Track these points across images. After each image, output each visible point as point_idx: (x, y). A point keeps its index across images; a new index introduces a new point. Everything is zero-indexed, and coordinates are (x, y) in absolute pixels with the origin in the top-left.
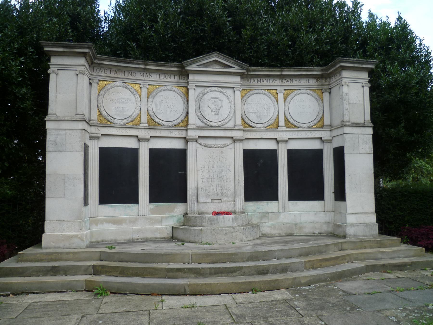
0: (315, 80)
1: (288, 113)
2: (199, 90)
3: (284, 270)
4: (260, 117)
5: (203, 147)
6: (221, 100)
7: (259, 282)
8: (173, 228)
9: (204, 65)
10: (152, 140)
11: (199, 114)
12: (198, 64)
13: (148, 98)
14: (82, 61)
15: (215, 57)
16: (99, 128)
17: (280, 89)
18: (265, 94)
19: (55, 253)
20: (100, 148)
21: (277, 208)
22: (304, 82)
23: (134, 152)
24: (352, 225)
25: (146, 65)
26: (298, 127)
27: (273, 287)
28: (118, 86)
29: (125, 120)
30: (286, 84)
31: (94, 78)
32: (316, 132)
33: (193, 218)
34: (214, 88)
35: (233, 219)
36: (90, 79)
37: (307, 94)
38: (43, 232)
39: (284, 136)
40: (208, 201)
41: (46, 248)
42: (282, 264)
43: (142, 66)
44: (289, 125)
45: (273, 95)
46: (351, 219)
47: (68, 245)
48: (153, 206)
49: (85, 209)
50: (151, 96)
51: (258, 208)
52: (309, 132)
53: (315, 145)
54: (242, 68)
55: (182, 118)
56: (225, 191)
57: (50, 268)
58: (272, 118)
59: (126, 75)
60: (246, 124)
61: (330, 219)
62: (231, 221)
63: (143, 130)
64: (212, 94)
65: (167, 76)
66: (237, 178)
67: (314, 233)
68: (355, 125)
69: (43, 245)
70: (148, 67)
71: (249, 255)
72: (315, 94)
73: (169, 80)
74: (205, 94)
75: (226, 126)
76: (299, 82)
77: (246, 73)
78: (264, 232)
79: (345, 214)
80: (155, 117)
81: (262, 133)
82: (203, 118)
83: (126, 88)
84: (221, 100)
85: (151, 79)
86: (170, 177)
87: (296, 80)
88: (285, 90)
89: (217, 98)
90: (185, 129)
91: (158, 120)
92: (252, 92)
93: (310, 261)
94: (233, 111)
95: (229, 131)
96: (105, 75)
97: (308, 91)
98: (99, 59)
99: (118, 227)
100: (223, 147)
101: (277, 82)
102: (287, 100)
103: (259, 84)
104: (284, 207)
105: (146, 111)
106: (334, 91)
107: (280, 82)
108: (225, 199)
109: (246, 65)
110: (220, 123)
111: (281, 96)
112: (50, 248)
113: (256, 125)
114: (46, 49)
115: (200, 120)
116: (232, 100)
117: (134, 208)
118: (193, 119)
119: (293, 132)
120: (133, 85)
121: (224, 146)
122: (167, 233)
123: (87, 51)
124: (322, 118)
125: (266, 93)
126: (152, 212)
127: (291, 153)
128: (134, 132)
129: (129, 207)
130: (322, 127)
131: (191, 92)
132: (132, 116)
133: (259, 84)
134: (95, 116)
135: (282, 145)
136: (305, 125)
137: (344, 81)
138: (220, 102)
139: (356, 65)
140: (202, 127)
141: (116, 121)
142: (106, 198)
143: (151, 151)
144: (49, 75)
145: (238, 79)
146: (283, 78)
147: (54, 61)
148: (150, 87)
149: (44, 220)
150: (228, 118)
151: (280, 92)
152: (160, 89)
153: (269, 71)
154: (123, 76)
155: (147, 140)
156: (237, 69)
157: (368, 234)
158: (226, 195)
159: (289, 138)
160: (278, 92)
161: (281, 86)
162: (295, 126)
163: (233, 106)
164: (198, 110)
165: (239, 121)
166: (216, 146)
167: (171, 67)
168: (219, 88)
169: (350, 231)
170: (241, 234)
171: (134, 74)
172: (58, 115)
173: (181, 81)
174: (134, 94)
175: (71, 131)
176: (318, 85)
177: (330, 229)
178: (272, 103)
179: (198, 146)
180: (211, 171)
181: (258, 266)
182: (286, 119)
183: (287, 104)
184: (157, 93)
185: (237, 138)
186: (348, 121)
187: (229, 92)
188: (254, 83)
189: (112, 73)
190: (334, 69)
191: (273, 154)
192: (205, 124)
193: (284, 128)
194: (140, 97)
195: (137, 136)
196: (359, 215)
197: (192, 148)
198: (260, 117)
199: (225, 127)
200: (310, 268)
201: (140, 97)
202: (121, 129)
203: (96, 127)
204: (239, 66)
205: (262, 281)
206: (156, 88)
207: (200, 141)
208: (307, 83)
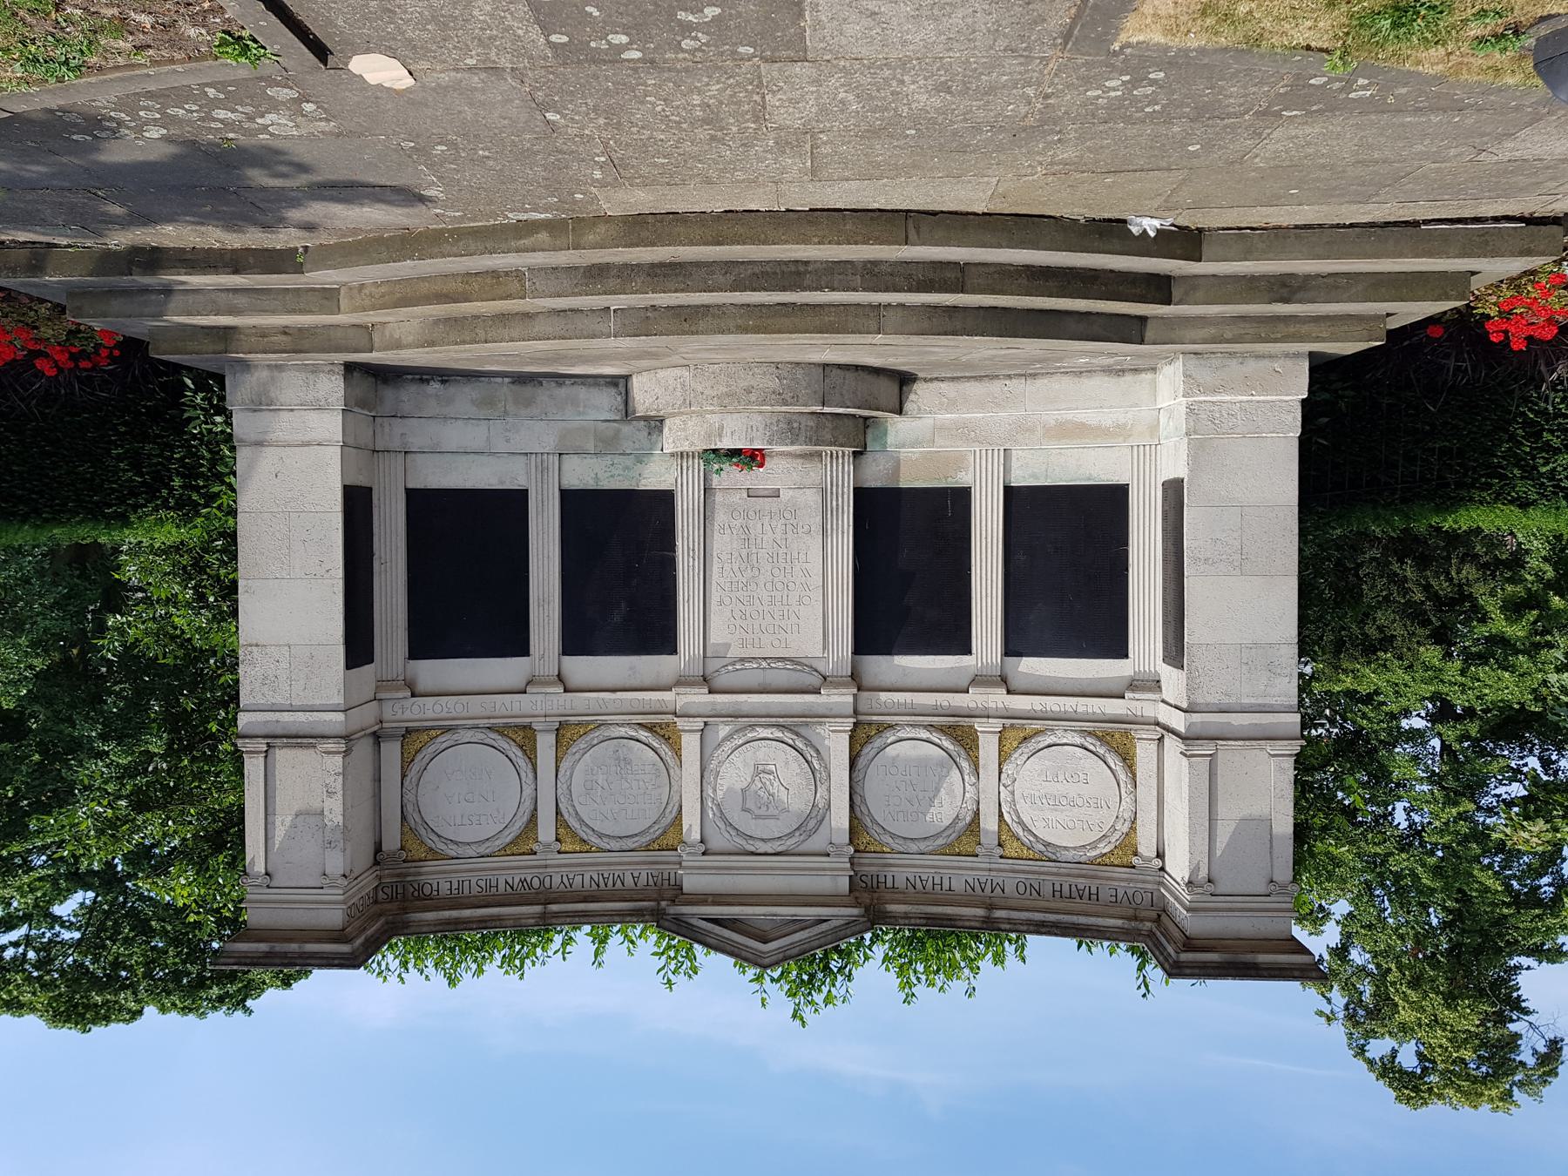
1: (523, 775)
2: (817, 842)
3: (596, 276)
4: (618, 759)
7: (691, 243)
8: (900, 411)
9: (799, 925)
12: (824, 927)
18: (600, 836)
19: (1276, 341)
20: (1127, 656)
21: (565, 467)
27: (639, 227)
29: (1049, 741)
32: (430, 714)
33: (841, 440)
34: (770, 851)
36: (1162, 869)
37: (456, 843)
41: (1297, 355)
42: (605, 293)
45: (574, 834)
46: (330, 425)
47: (1233, 363)
48: (962, 479)
49: (1181, 472)
50: (968, 819)
51: (627, 468)
52: (454, 714)
53: (432, 671)
55: (868, 751)
56: (737, 523)
57: (1298, 296)
61: (387, 430)
62: (727, 431)
64: (774, 828)
66: (698, 564)
67: (443, 382)
69: (1306, 365)
71: (702, 325)
73: (910, 873)
76: (482, 883)
77: (663, 904)
78: (613, 391)
79: (345, 445)
85: (970, 876)
86: (904, 567)
87: (494, 890)
89: (758, 817)
90: (861, 718)
91: (946, 743)
92: (644, 839)
93: (506, 298)
99: (1070, 417)
104: (544, 470)
105: (981, 771)
106: (366, 857)
111: (546, 832)
112: (1287, 355)
118: (837, 745)
122: (920, 395)
123: (1184, 957)
124: (406, 764)
127: (518, 645)
129: (1034, 476)
130: (408, 731)
136: (468, 735)
137: (336, 895)
139: (294, 947)
141: (1078, 740)
142: (1107, 504)
145: (691, 883)
149: (1304, 442)
152: (940, 841)
155: (979, 680)
160: (558, 846)
162: (501, 734)
165: (690, 743)
168: (752, 849)
170: (700, 389)
176: (420, 874)
177: (389, 393)
180: (780, 586)
181: (682, 291)
182: (530, 754)
183: (527, 806)
189: (1094, 890)
190: (369, 932)
191: (576, 641)
192: (797, 734)
194: (1001, 815)
195: (1009, 692)
196: (300, 437)
200: (507, 274)
205: (681, 244)
206: (951, 845)
207: (815, 680)
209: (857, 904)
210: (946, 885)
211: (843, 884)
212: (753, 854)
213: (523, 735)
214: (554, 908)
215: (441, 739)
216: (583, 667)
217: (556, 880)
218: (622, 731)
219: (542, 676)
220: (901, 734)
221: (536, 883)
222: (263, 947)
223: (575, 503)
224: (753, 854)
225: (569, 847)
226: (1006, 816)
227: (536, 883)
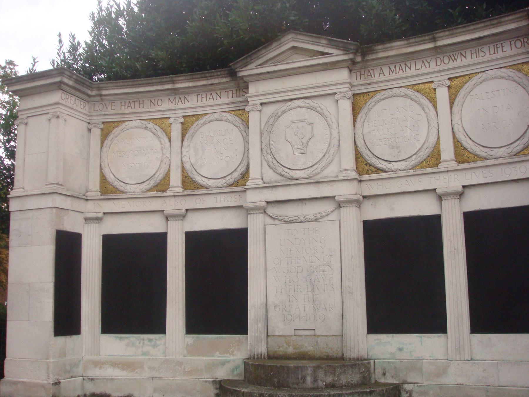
0: (519, 44)
1: (461, 130)
2: (269, 110)
4: (397, 147)
5: (277, 222)
6: (311, 124)
10: (190, 215)
11: (269, 157)
12: (259, 62)
13: (183, 140)
14: (56, 97)
15: (290, 41)
16: (100, 202)
17: (439, 79)
18: (406, 96)
22: (492, 52)
23: (159, 241)
25: (173, 82)
28: (132, 128)
30: (452, 64)
31: (95, 119)
34: (295, 101)
37: (502, 78)
44: (462, 155)
45: (425, 94)
48: (192, 338)
50: (187, 136)
54: (346, 50)
58: (425, 147)
60: (370, 165)
63: (173, 199)
64: (292, 116)
65: (214, 95)
72: (520, 75)
73: (219, 101)
74: (279, 117)
76: (482, 54)
80: (195, 172)
81: (404, 180)
82: (277, 164)
83: (146, 128)
84: (311, 124)
85: (188, 105)
87: (473, 51)
89: (303, 121)
91: (199, 179)
92: (378, 96)
94: (336, 143)
95: (326, 184)
96: (114, 112)
97: (502, 70)
100: (316, 220)
102: (457, 100)
103: (394, 76)
104: (459, 349)
107: (439, 63)
111: (442, 94)
113: (390, 166)
115: (272, 168)
116: (334, 120)
117: (158, 342)
119: (473, 171)
120: (158, 121)
121: (318, 216)
123: (58, 79)
125: (409, 92)
126: (191, 350)
127: (474, 221)
131: (254, 118)
132: (156, 176)
134: (95, 185)
135: (448, 203)
138: (309, 128)
140: (276, 182)
141: (128, 188)
142: (112, 324)
145: (343, 75)
148: (187, 119)
150: (326, 157)
151: (440, 85)
156: (337, 55)
159: (464, 187)
161: (440, 71)
163: (335, 133)
164: (267, 150)
165: (348, 162)
166: (302, 219)
168: (306, 101)
171: (160, 101)
173: (239, 99)
174: (159, 137)
175: (39, 212)
178: (422, 112)
179: (269, 220)
182: (457, 143)
183: (456, 109)
184: (198, 130)
185: (343, 198)
187: (327, 104)
188: (382, 78)
189: (123, 107)
193: (453, 165)
194: (170, 141)
197: (255, 226)
198: (398, 147)
199: (322, 178)
201: (170, 141)
202: (135, 200)
203: (96, 202)
204: (337, 47)
207: (271, 210)
208: (500, 54)
209: (242, 78)
210: (199, 98)
211: (252, 89)
212: (306, 98)
215: (519, 148)
216: (424, 207)
217: (433, 64)
218: (395, 166)
220: (222, 181)
223: (436, 324)
224: (306, 98)
225: (427, 86)
226: (167, 140)
227: (446, 60)
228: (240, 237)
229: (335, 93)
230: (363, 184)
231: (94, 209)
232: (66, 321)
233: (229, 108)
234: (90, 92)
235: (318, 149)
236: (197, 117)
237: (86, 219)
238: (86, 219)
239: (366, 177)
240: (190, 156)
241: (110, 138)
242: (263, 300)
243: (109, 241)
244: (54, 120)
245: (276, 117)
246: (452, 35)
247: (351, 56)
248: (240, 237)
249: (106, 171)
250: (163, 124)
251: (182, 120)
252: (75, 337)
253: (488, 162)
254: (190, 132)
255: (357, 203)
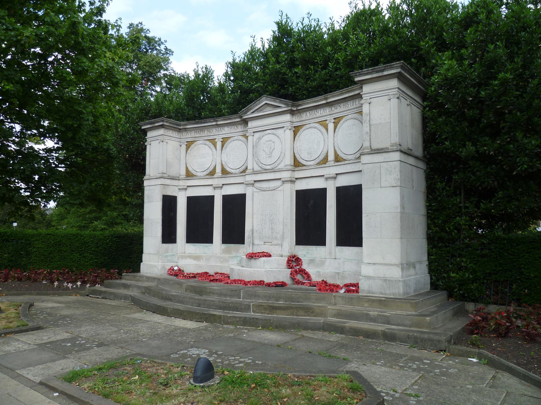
2: (257, 135)
10: (224, 186)
14: (161, 131)
15: (264, 100)
18: (315, 128)
24: (368, 277)
25: (217, 121)
26: (345, 160)
30: (336, 111)
31: (183, 140)
35: (264, 262)
37: (355, 119)
38: (142, 261)
39: (331, 173)
40: (261, 243)
43: (214, 123)
51: (308, 253)
54: (287, 105)
59: (206, 133)
64: (266, 138)
68: (374, 152)
70: (219, 123)
75: (279, 167)
76: (347, 106)
84: (274, 142)
88: (334, 119)
89: (271, 141)
91: (228, 169)
92: (304, 128)
97: (355, 114)
98: (183, 125)
101: (327, 111)
104: (330, 253)
108: (275, 242)
109: (290, 102)
110: (273, 166)
111: (331, 126)
114: (143, 128)
123: (161, 123)
126: (225, 251)
128: (209, 182)
129: (207, 246)
131: (250, 138)
133: (311, 117)
134: (183, 172)
138: (273, 144)
141: (198, 174)
142: (191, 238)
143: (224, 197)
144: (146, 146)
145: (287, 117)
146: (332, 105)
147: (150, 134)
149: (142, 252)
153: (315, 102)
154: (204, 135)
157: (387, 292)
158: (276, 238)
159: (337, 174)
161: (330, 115)
167: (235, 118)
169: (364, 286)
172: (151, 175)
174: (211, 149)
179: (255, 190)
186: (367, 148)
187: (280, 131)
193: (332, 163)
196: (377, 267)
197: (249, 192)
207: (257, 185)
211: (251, 124)
213: (338, 159)
214: (324, 102)
217: (328, 111)
219: (328, 182)
221: (333, 109)
222: (386, 73)
225: (324, 122)
228: (242, 197)
229: (284, 127)
230: (296, 172)
231: (183, 183)
232: (169, 236)
233: (242, 134)
234: (179, 127)
235: (276, 155)
236: (228, 138)
237: (179, 189)
238: (179, 189)
239: (297, 169)
240: (225, 159)
241: (190, 149)
242: (251, 228)
243: (190, 200)
244: (161, 143)
245: (260, 139)
246: (333, 97)
247: (290, 108)
248: (242, 197)
249: (188, 166)
250: (213, 142)
251: (222, 140)
252: (174, 245)
253: (347, 162)
254: (225, 146)
255: (292, 182)
